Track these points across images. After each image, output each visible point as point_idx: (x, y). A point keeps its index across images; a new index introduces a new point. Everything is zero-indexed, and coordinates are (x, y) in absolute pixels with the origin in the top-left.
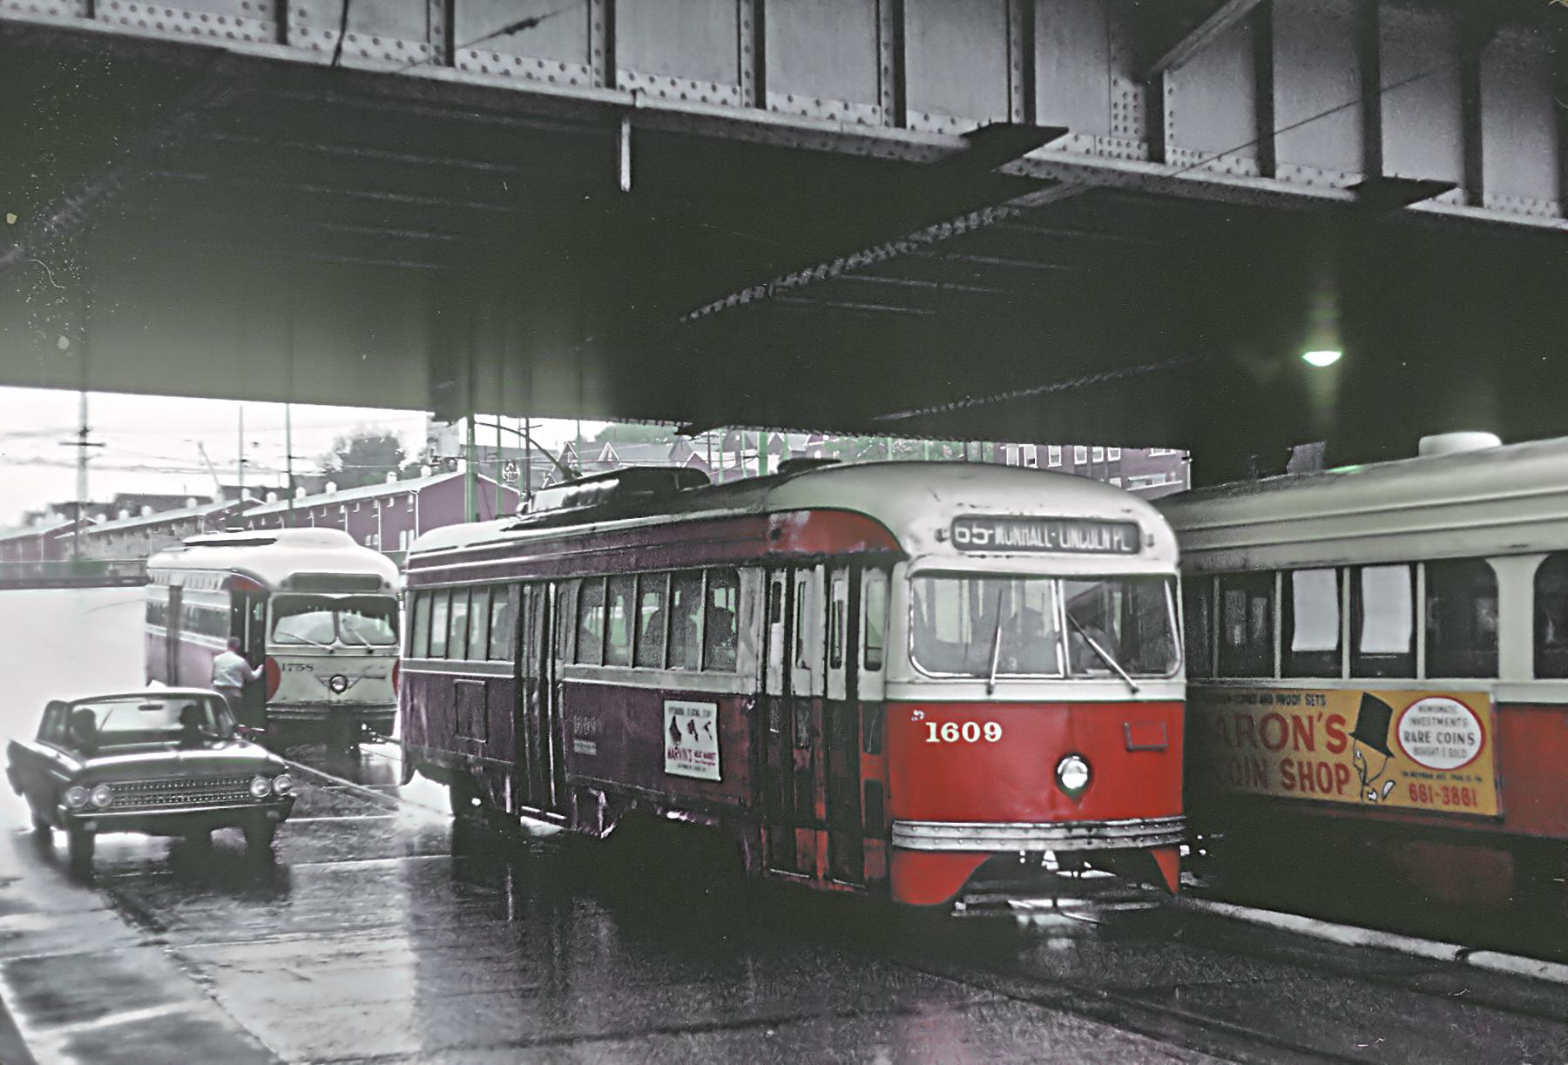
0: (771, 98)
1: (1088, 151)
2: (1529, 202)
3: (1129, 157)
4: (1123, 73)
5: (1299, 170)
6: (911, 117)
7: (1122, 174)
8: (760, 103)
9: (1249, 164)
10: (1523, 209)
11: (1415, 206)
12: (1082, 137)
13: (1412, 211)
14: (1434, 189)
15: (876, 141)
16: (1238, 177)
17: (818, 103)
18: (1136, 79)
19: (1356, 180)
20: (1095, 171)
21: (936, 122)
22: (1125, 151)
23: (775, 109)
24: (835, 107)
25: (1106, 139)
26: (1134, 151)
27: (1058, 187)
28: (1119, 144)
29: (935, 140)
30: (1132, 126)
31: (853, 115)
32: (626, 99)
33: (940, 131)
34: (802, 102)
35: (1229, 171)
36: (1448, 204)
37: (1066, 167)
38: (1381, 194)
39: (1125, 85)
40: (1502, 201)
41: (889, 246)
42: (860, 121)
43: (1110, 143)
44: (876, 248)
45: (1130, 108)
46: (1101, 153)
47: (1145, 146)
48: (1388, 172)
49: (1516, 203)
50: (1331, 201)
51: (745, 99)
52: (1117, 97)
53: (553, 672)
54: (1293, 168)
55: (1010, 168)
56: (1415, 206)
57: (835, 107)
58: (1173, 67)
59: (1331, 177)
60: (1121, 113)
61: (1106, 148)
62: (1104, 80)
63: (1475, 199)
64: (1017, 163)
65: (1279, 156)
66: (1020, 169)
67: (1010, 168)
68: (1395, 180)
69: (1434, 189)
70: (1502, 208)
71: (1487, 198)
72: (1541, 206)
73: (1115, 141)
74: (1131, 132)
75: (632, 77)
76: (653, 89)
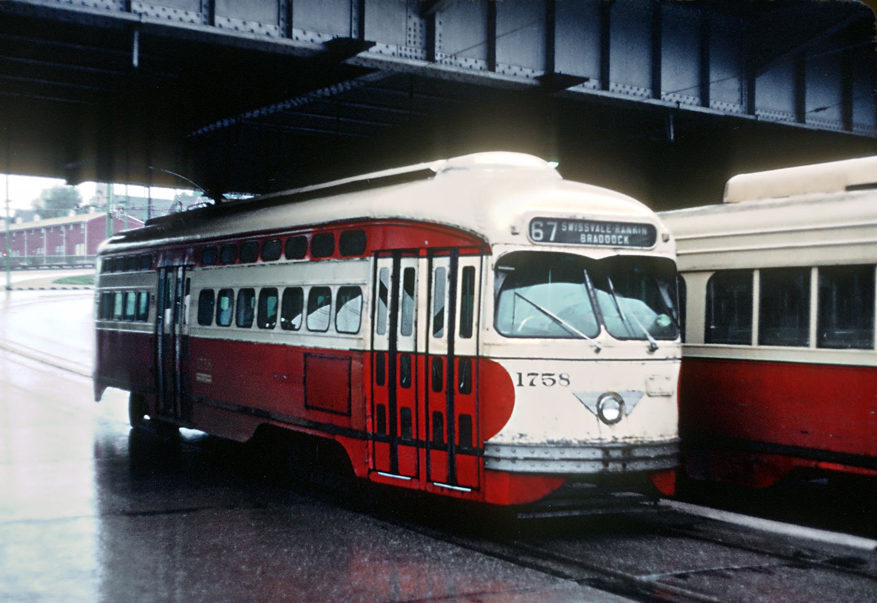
0: (218, 19)
1: (393, 54)
2: (635, 89)
3: (416, 58)
4: (415, 12)
5: (509, 68)
6: (296, 32)
7: (411, 67)
8: (212, 22)
9: (481, 63)
10: (631, 92)
11: (572, 89)
12: (390, 46)
13: (569, 92)
14: (582, 80)
15: (276, 45)
16: (509, 76)
17: (244, 23)
18: (421, 15)
19: (539, 73)
20: (397, 64)
21: (310, 35)
22: (413, 54)
23: (220, 26)
24: (254, 25)
25: (403, 48)
26: (419, 54)
27: (379, 72)
28: (411, 50)
29: (309, 45)
30: (418, 40)
31: (263, 31)
32: (135, 18)
33: (312, 41)
34: (236, 22)
35: (471, 67)
36: (590, 87)
37: (381, 62)
38: (553, 83)
39: (415, 19)
40: (620, 87)
41: (296, 104)
42: (268, 34)
43: (406, 50)
44: (301, 103)
45: (418, 31)
46: (401, 55)
47: (425, 52)
48: (557, 70)
49: (628, 88)
50: (525, 85)
51: (204, 20)
52: (411, 26)
53: (13, 361)
54: (507, 66)
55: (351, 61)
56: (572, 89)
57: (254, 25)
58: (442, 11)
59: (528, 72)
60: (412, 33)
61: (403, 52)
62: (404, 18)
63: (605, 85)
64: (355, 59)
65: (498, 59)
66: (357, 62)
67: (351, 61)
68: (560, 74)
69: (582, 80)
70: (628, 93)
71: (612, 86)
72: (642, 91)
73: (408, 49)
74: (418, 44)
75: (141, 6)
76: (152, 13)
